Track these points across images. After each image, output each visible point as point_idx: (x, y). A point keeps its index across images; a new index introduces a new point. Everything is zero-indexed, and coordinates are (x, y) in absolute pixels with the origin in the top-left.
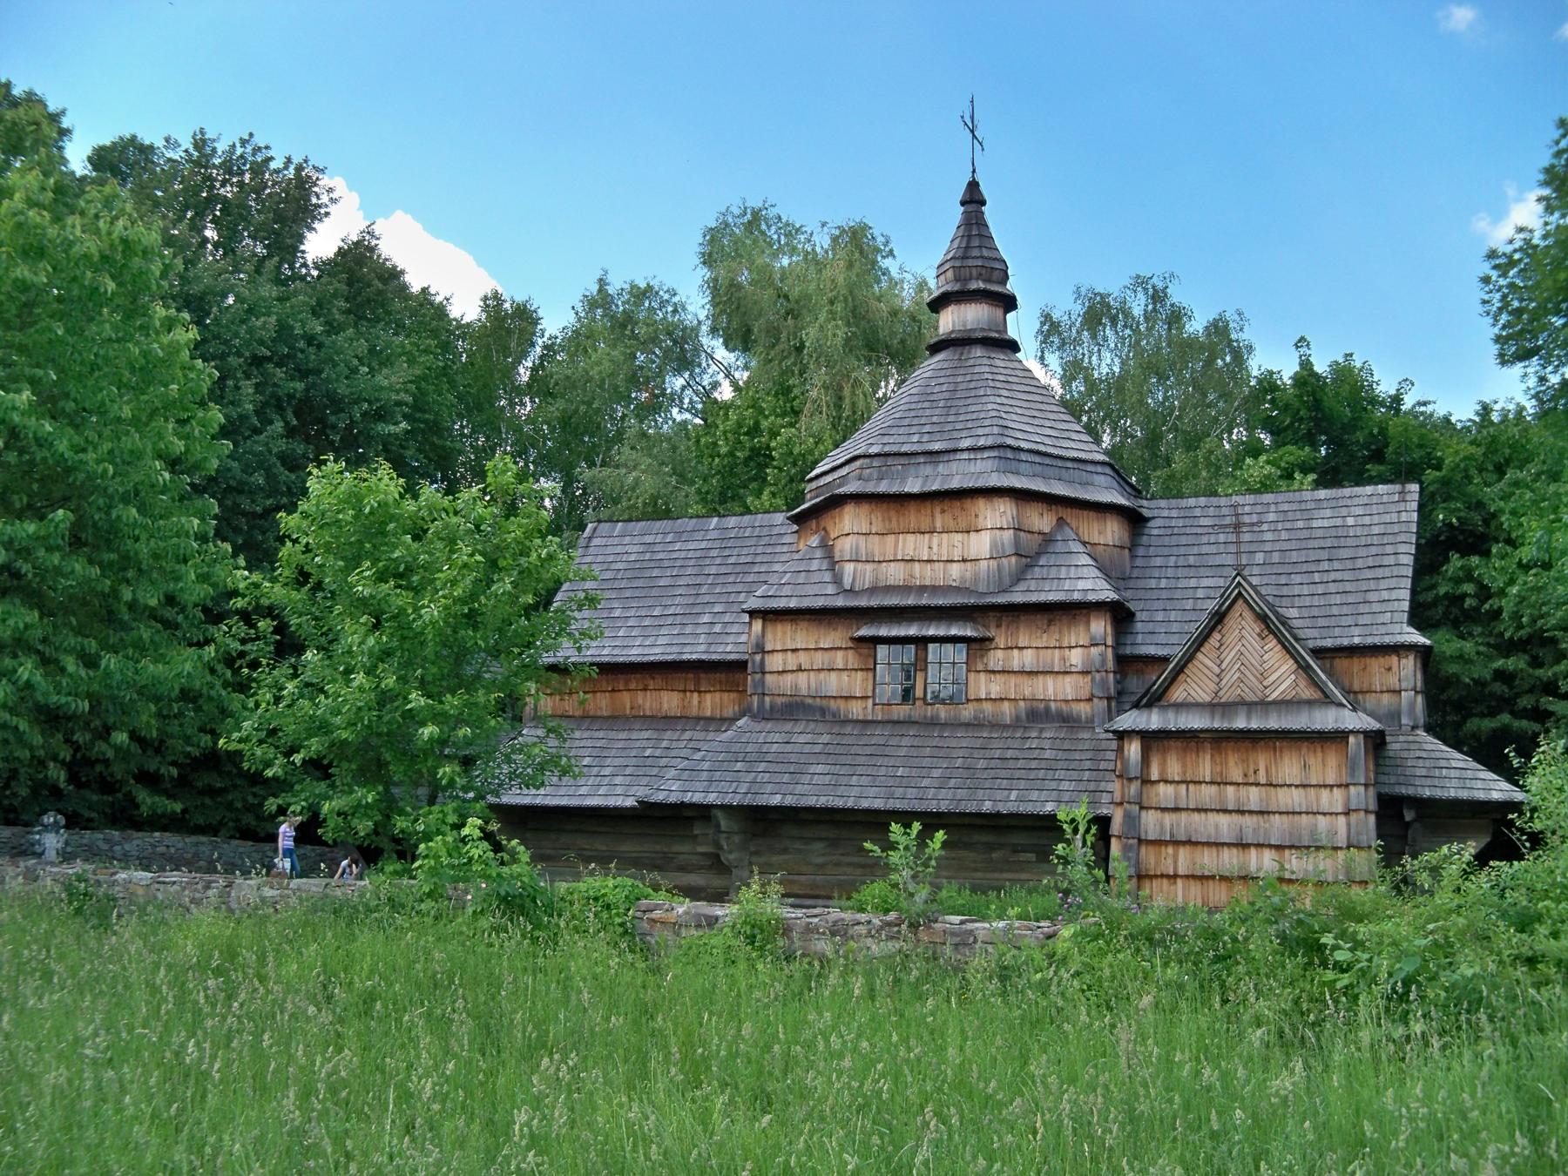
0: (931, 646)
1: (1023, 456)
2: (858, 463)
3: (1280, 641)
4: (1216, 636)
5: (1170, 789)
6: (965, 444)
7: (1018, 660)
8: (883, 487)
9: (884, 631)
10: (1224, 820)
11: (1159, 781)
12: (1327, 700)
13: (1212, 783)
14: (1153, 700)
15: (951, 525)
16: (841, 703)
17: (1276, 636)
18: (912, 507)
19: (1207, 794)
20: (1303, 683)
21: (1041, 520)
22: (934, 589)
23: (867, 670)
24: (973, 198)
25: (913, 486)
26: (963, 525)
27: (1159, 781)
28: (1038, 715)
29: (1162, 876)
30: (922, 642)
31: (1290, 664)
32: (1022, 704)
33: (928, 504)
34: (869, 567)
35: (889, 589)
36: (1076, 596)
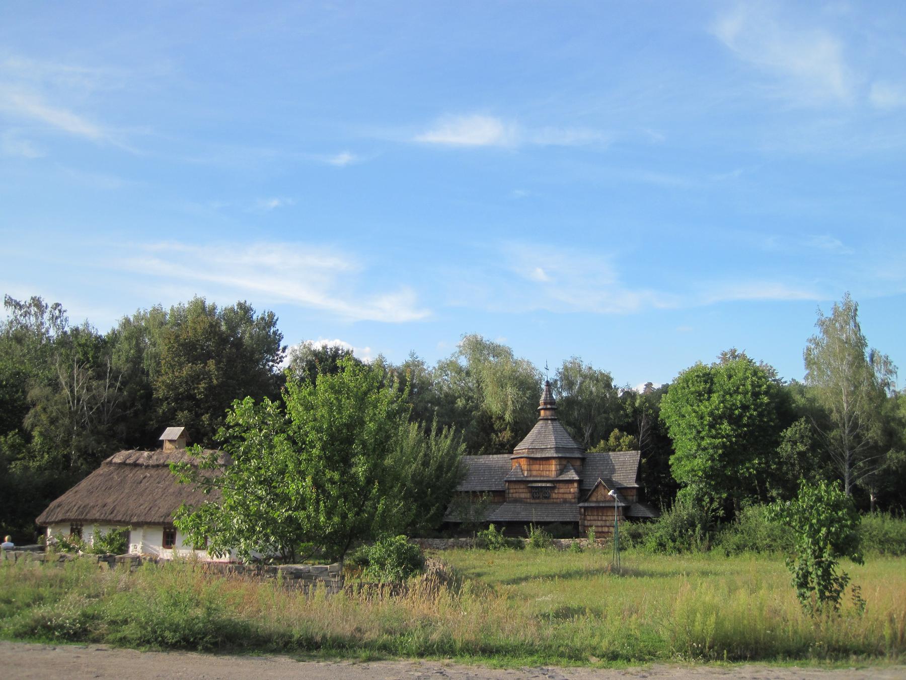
6: (549, 447)
8: (532, 456)
14: (586, 501)
19: (596, 518)
21: (564, 462)
25: (539, 455)
28: (565, 501)
35: (534, 476)
36: (571, 478)
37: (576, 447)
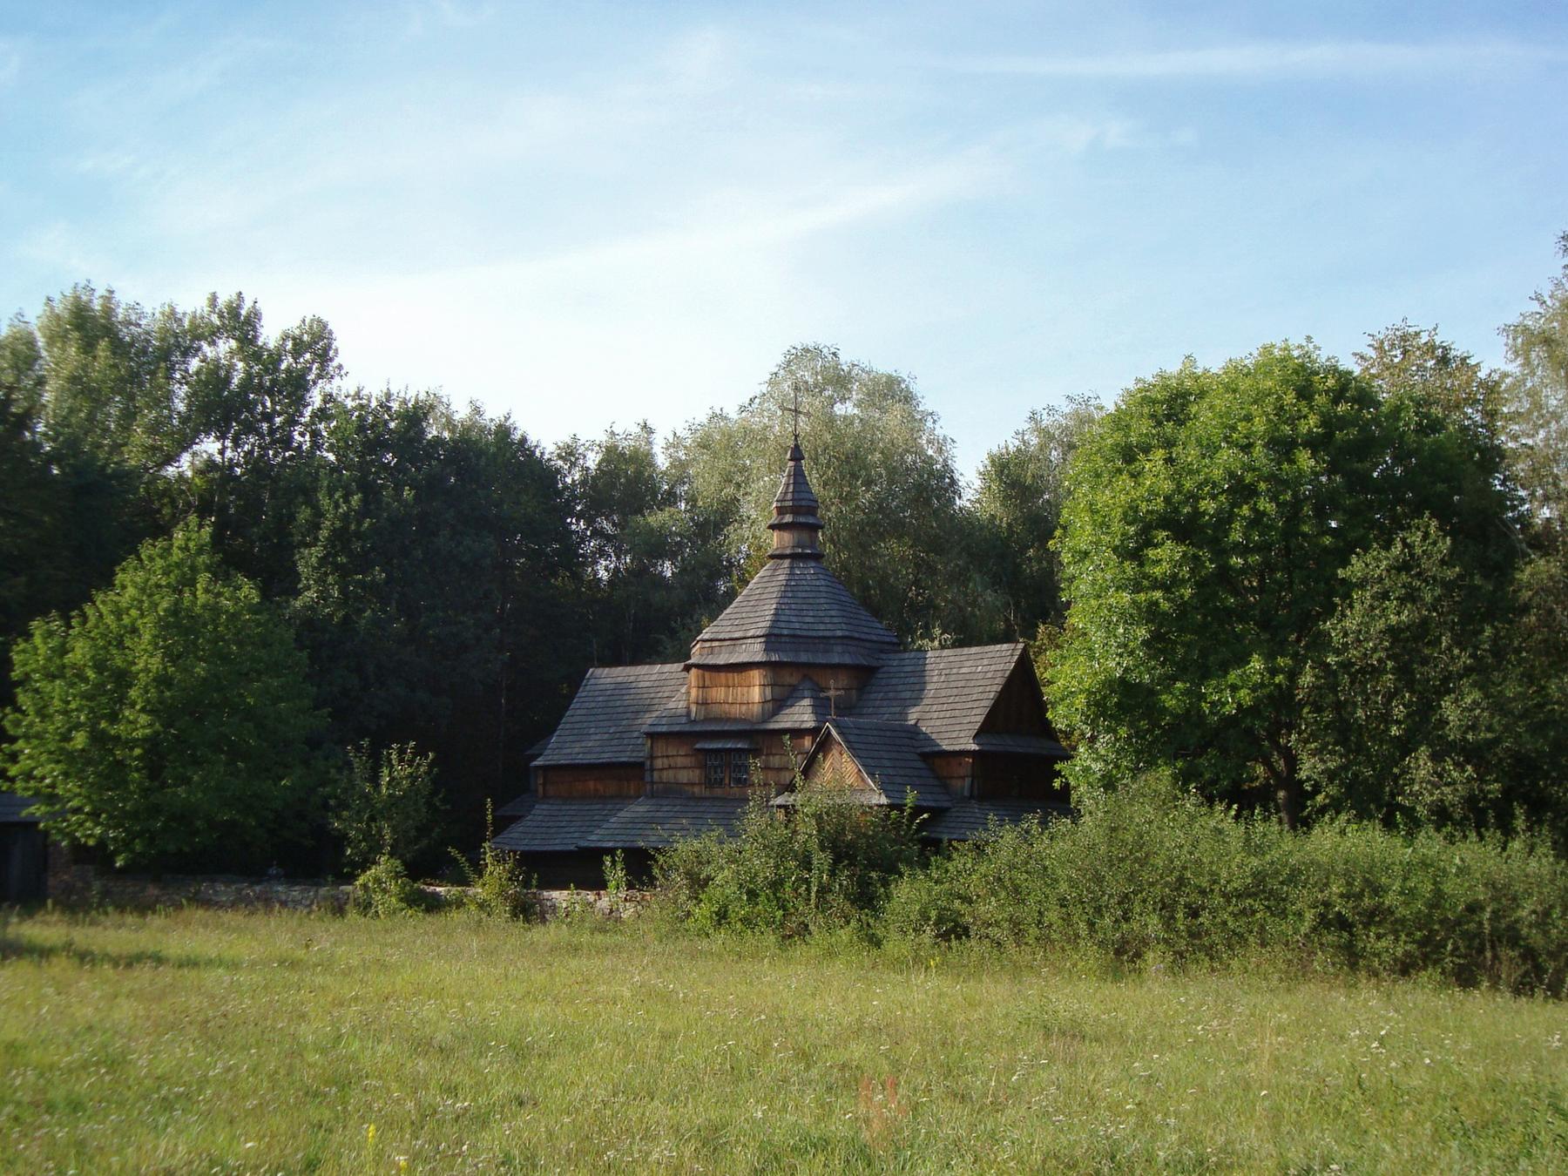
1: (783, 639)
6: (750, 634)
21: (790, 678)
25: (721, 660)
36: (797, 725)
37: (839, 633)
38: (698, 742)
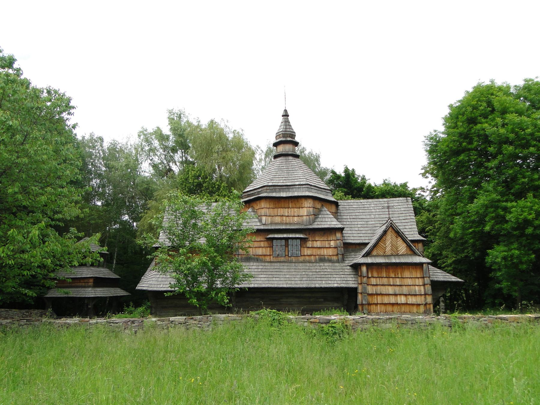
0: (289, 240)
2: (265, 188)
3: (402, 239)
4: (385, 237)
5: (374, 279)
7: (318, 244)
9: (276, 236)
10: (390, 288)
11: (371, 277)
12: (415, 254)
13: (386, 277)
15: (294, 206)
16: (263, 257)
17: (401, 237)
18: (282, 200)
19: (385, 281)
20: (408, 250)
21: (318, 205)
22: (290, 224)
23: (271, 247)
24: (286, 115)
26: (298, 206)
27: (371, 277)
29: (374, 304)
30: (287, 239)
31: (405, 245)
32: (317, 257)
33: (287, 200)
34: (270, 218)
35: (276, 224)
36: (332, 226)
38: (268, 235)
